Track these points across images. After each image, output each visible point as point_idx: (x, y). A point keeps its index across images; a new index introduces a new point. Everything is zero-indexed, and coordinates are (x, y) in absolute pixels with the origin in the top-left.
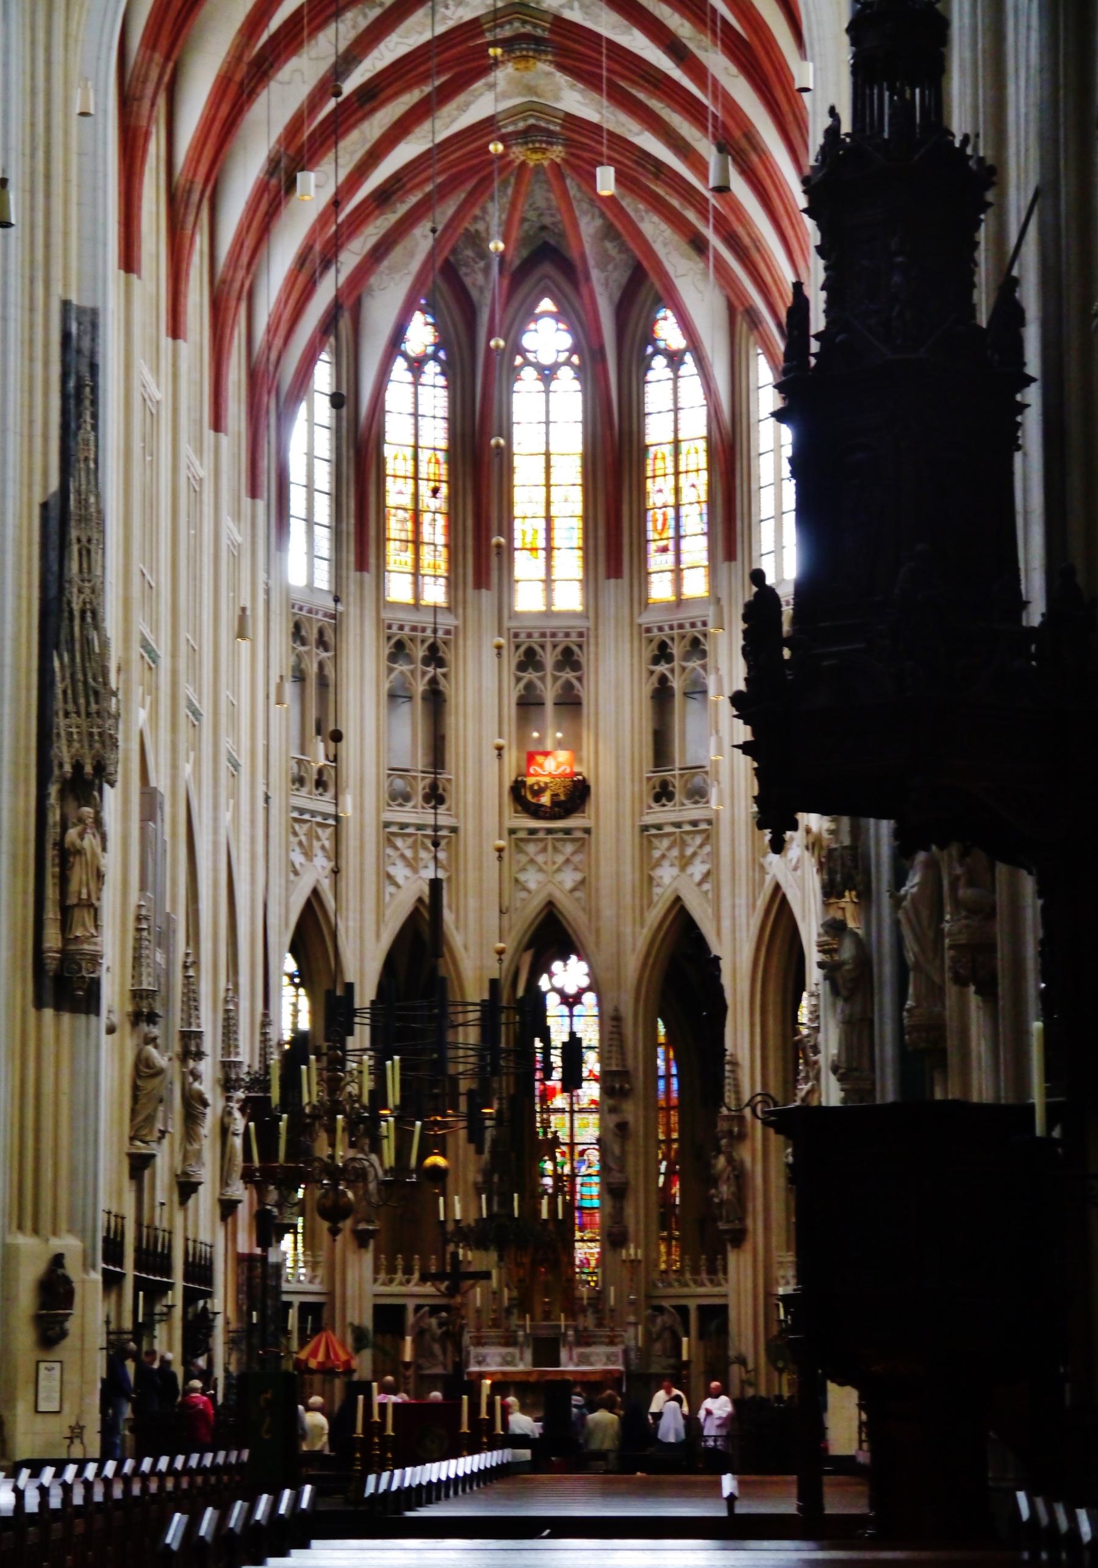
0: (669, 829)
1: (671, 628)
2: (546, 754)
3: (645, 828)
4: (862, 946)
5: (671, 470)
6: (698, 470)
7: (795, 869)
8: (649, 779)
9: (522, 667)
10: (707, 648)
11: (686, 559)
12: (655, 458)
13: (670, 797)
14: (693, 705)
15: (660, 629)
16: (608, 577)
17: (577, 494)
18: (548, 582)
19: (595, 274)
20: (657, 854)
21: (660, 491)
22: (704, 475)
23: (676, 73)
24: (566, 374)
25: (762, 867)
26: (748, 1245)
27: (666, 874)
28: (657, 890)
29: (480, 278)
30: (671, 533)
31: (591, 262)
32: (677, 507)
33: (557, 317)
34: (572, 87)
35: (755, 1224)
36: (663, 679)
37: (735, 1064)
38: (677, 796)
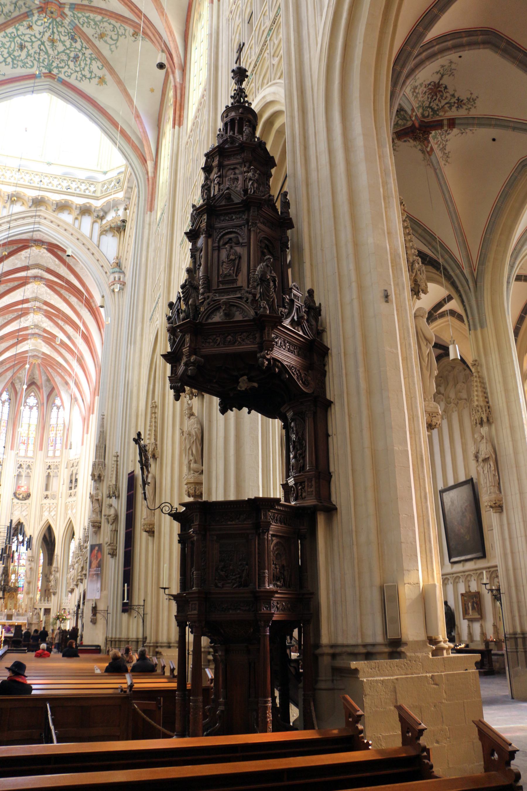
2: (22, 487)
4: (116, 511)
5: (55, 429)
9: (19, 468)
11: (57, 448)
13: (48, 498)
14: (55, 479)
17: (34, 433)
18: (26, 451)
19: (44, 388)
20: (44, 509)
24: (35, 408)
26: (57, 595)
27: (46, 514)
28: (44, 518)
29: (19, 386)
30: (54, 443)
31: (43, 386)
32: (56, 438)
33: (35, 396)
34: (45, 346)
35: (59, 591)
36: (49, 473)
37: (57, 556)
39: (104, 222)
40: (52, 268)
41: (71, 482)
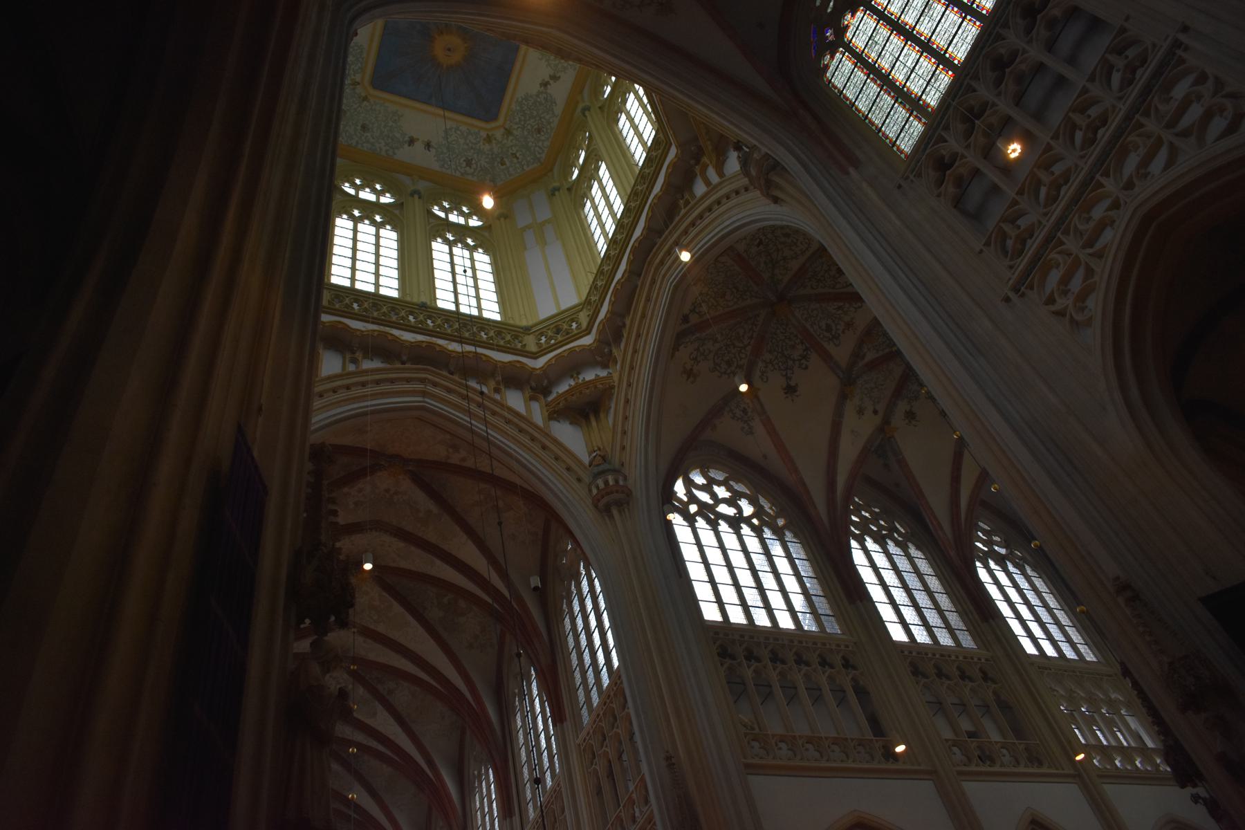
23: (381, 748)
39: (550, 398)
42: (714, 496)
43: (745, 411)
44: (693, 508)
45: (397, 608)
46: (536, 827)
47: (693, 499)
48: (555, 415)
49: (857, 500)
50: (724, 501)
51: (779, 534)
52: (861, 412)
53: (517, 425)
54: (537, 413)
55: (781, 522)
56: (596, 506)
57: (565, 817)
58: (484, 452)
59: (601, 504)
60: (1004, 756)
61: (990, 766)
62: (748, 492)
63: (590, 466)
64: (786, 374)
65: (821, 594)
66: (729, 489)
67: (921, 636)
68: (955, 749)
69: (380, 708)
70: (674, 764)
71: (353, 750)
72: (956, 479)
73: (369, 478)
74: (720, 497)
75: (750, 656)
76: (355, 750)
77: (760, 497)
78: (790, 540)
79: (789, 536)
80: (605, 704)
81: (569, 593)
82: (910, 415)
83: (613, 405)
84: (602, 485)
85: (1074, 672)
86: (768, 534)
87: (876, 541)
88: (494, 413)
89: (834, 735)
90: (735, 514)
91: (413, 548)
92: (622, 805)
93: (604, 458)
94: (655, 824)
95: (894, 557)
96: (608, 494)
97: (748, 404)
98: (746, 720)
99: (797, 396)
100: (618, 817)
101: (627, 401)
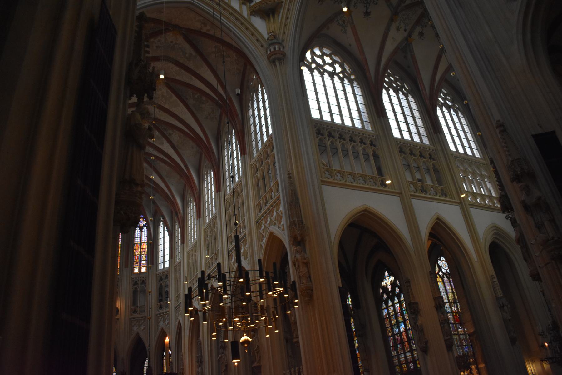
0: (136, 319)
1: (138, 278)
3: (130, 319)
6: (145, 248)
7: (167, 325)
8: (132, 308)
10: (146, 282)
12: (136, 246)
13: (136, 312)
15: (136, 278)
16: (125, 268)
21: (137, 252)
22: (146, 249)
25: (158, 325)
27: (135, 328)
32: (141, 255)
36: (136, 288)
38: (138, 313)
39: (252, 4)
40: (181, 61)
41: (160, 294)
42: (324, 61)
43: (344, 22)
44: (313, 66)
45: (174, 98)
46: (230, 197)
47: (314, 61)
48: (254, 13)
49: (389, 71)
50: (328, 64)
51: (351, 82)
52: (398, 29)
53: (235, 16)
54: (245, 11)
55: (353, 77)
56: (269, 59)
57: (243, 194)
58: (219, 28)
59: (271, 59)
60: (431, 191)
61: (425, 194)
62: (340, 61)
63: (268, 40)
64: (366, 6)
65: (366, 112)
66: (331, 58)
67: (407, 136)
68: (412, 186)
69: (165, 141)
70: (291, 177)
71: (153, 158)
72: (436, 68)
73: (163, 35)
74: (326, 62)
75: (330, 135)
76: (154, 158)
77: (345, 64)
78: (356, 86)
79: (355, 84)
80: (264, 149)
81: (253, 99)
82: (421, 34)
83: (282, 11)
84: (272, 50)
85: (469, 160)
86: (346, 81)
87: (394, 91)
88: (224, 9)
89: (361, 173)
90: (332, 71)
91: (183, 71)
92: (267, 191)
93: (275, 37)
94: (280, 201)
95: (401, 99)
96: (275, 54)
97: (346, 18)
98: (325, 162)
99: (370, 17)
100: (265, 196)
101: (289, 10)
